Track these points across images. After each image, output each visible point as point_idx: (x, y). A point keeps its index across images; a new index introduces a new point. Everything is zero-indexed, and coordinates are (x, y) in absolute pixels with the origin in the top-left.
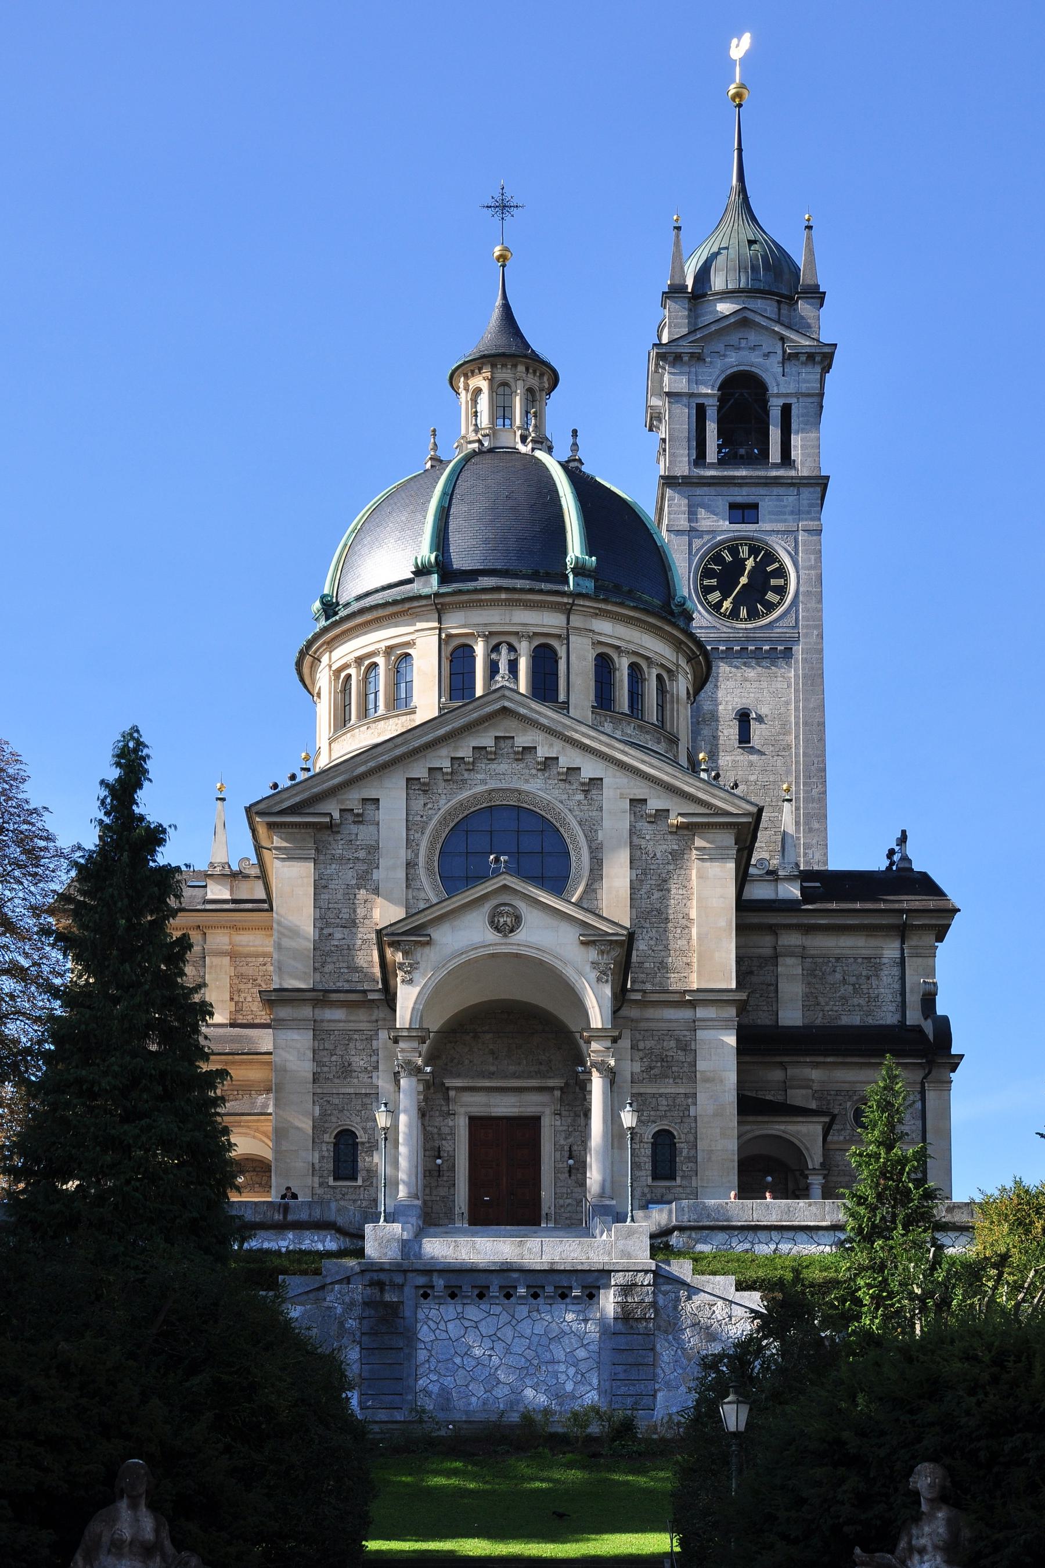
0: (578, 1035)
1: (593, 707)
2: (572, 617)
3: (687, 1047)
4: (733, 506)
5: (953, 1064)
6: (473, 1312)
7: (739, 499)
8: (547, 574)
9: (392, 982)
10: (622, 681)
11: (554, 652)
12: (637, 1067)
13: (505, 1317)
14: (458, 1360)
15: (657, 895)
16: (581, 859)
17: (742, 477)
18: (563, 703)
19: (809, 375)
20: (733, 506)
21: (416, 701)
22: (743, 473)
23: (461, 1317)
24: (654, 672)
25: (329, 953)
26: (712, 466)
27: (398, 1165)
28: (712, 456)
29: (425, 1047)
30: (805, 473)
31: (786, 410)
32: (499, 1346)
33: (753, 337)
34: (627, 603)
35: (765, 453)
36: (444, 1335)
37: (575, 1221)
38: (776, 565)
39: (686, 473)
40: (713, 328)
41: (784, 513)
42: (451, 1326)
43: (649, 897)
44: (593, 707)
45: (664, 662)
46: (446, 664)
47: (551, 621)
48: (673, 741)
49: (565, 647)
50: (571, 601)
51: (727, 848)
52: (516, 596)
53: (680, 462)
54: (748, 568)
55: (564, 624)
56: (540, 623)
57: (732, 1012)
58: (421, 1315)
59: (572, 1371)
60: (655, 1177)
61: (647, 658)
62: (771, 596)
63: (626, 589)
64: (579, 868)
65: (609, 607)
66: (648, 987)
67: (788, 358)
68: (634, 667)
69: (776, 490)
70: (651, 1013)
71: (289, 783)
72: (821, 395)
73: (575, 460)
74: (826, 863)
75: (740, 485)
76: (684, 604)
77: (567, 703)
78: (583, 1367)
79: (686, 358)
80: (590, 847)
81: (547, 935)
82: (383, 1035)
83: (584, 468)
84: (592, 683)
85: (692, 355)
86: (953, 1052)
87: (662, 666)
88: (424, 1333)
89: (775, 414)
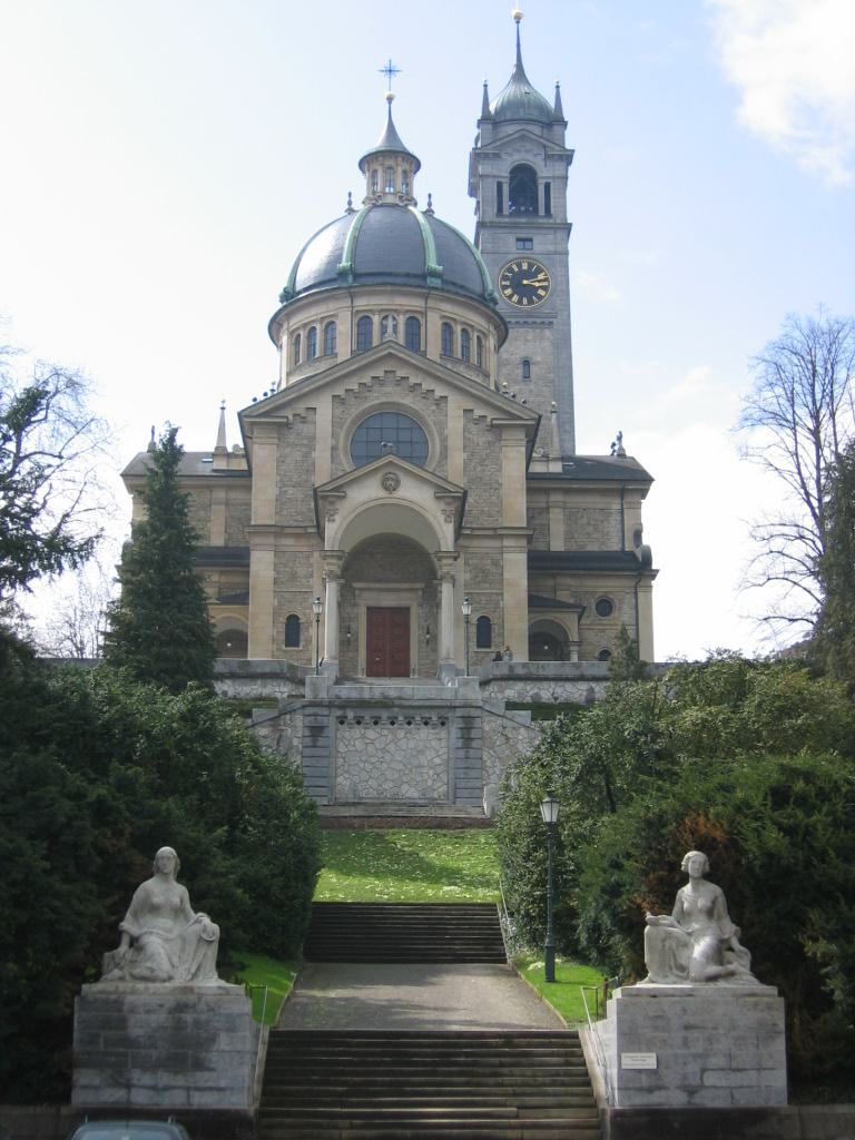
0: (433, 556)
3: (496, 564)
5: (653, 574)
6: (371, 734)
7: (522, 236)
9: (322, 523)
11: (418, 320)
12: (468, 576)
13: (390, 737)
14: (362, 765)
15: (479, 469)
16: (435, 447)
19: (558, 169)
20: (518, 240)
21: (337, 350)
22: (523, 220)
23: (363, 737)
24: (476, 334)
26: (506, 217)
27: (325, 639)
28: (506, 211)
29: (341, 563)
30: (558, 221)
31: (547, 186)
32: (388, 757)
33: (528, 146)
35: (536, 210)
36: (353, 749)
37: (432, 672)
40: (506, 140)
42: (357, 743)
46: (355, 329)
47: (416, 303)
48: (487, 376)
51: (522, 440)
57: (524, 542)
58: (339, 736)
59: (431, 772)
60: (479, 646)
61: (472, 326)
66: (474, 526)
67: (548, 157)
68: (463, 330)
70: (476, 543)
71: (263, 398)
72: (567, 178)
74: (574, 451)
78: (439, 770)
81: (413, 493)
82: (316, 554)
83: (435, 216)
86: (654, 567)
87: (480, 331)
88: (342, 748)
89: (541, 189)
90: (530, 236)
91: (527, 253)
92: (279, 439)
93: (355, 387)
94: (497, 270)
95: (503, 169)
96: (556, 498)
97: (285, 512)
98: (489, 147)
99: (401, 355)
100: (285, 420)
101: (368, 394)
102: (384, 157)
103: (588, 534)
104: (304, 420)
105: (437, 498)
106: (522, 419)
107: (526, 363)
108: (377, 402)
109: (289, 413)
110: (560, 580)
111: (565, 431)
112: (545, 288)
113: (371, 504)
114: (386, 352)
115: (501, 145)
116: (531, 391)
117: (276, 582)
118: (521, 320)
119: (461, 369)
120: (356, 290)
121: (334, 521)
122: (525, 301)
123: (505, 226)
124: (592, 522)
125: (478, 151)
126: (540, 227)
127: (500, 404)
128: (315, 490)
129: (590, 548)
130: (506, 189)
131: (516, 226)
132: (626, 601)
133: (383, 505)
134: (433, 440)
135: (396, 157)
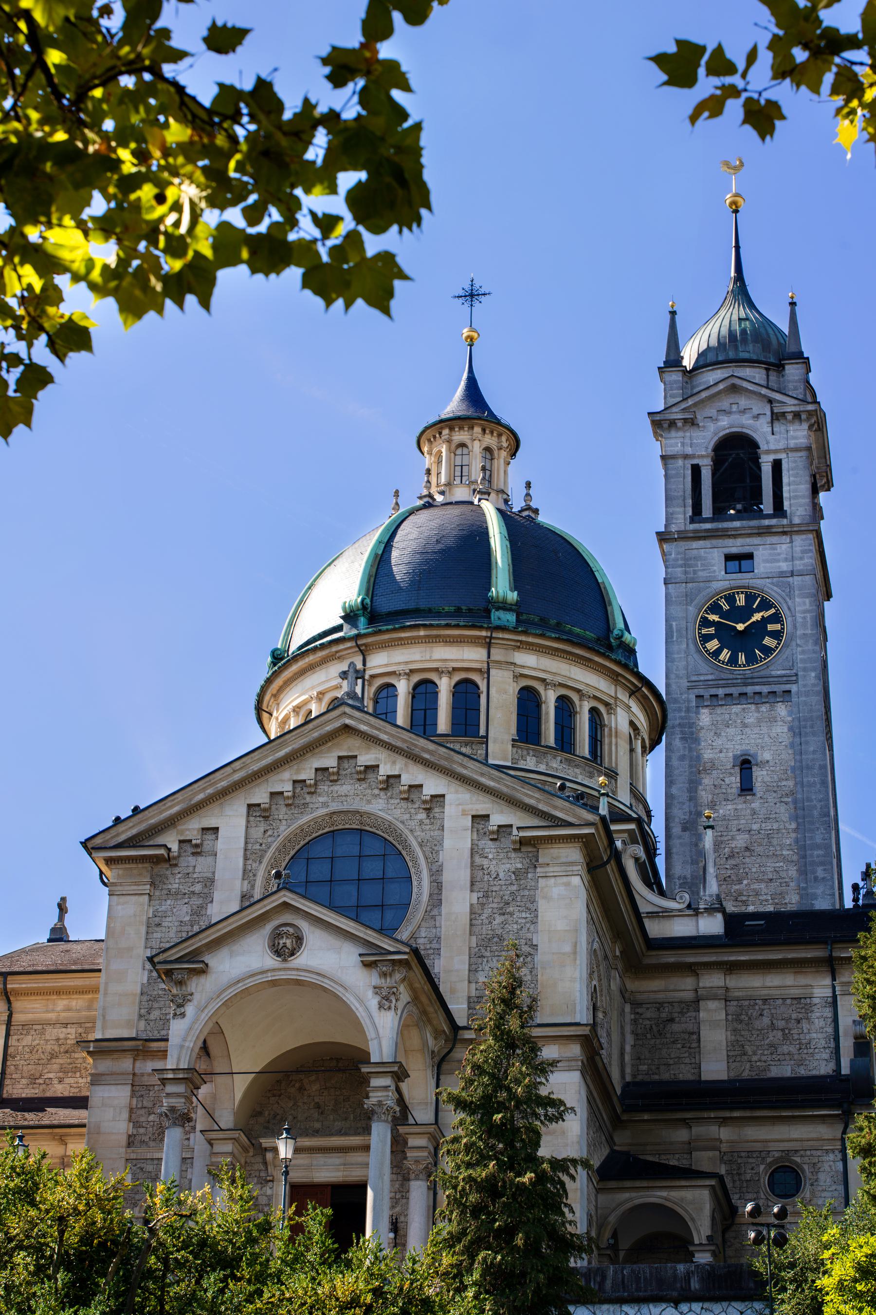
1: (513, 740)
2: (493, 651)
4: (729, 558)
7: (734, 550)
8: (470, 610)
10: (547, 713)
15: (499, 919)
16: (422, 887)
17: (736, 529)
18: (482, 737)
20: (729, 558)
24: (586, 706)
25: (155, 999)
26: (706, 520)
28: (707, 510)
34: (549, 634)
38: (773, 611)
39: (683, 528)
41: (778, 561)
43: (490, 923)
44: (513, 740)
45: (598, 694)
47: (471, 655)
48: (612, 775)
49: (485, 680)
50: (489, 634)
52: (434, 632)
53: (676, 519)
54: (754, 619)
55: (485, 658)
56: (460, 657)
61: (578, 691)
62: (768, 641)
63: (553, 622)
64: (420, 894)
65: (530, 639)
69: (770, 539)
73: (526, 510)
75: (734, 536)
76: (622, 636)
77: (486, 737)
79: (680, 424)
80: (430, 870)
83: (541, 519)
84: (514, 717)
85: (685, 420)
87: (595, 698)
90: (746, 550)
91: (743, 579)
92: (152, 884)
93: (287, 788)
94: (692, 609)
95: (700, 443)
96: (713, 980)
97: (155, 1014)
98: (674, 409)
99: (363, 728)
100: (162, 851)
101: (308, 798)
102: (452, 429)
103: (771, 1045)
104: (198, 850)
105: (367, 965)
106: (570, 825)
107: (745, 765)
108: (324, 811)
109: (171, 840)
110: (698, 1130)
111: (816, 879)
112: (777, 635)
113: (250, 982)
114: (337, 724)
115: (695, 405)
116: (754, 812)
117: (131, 1141)
118: (735, 691)
119: (556, 764)
120: (369, 640)
121: (183, 1015)
122: (742, 658)
123: (698, 536)
124: (781, 1024)
125: (658, 418)
126: (767, 531)
127: (532, 802)
129: (775, 1072)
131: (724, 534)
132: (826, 1167)
133: (274, 983)
134: (419, 873)
135: (472, 428)
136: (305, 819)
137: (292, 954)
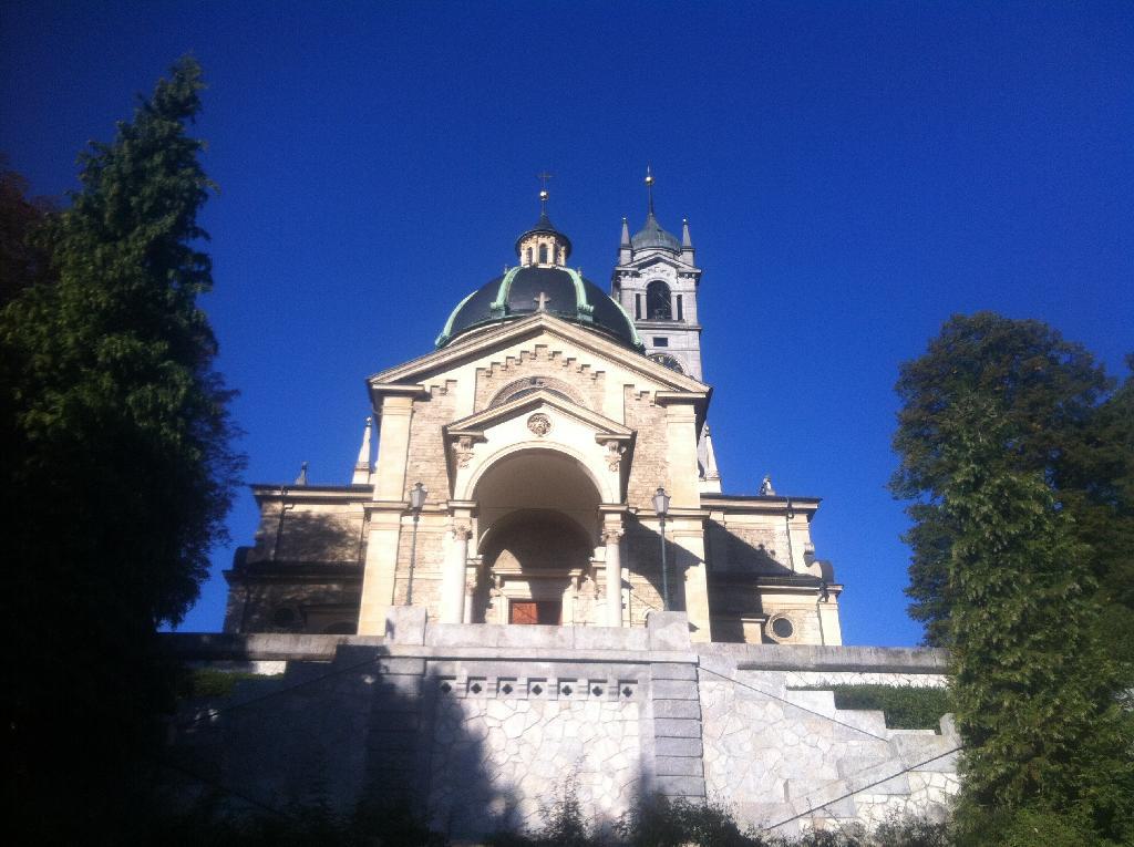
7: (658, 336)
31: (679, 297)
33: (661, 265)
57: (698, 525)
89: (674, 301)
90: (665, 336)
99: (553, 327)
101: (516, 368)
109: (427, 384)
128: (445, 429)
130: (643, 299)
136: (514, 379)
137: (544, 432)
